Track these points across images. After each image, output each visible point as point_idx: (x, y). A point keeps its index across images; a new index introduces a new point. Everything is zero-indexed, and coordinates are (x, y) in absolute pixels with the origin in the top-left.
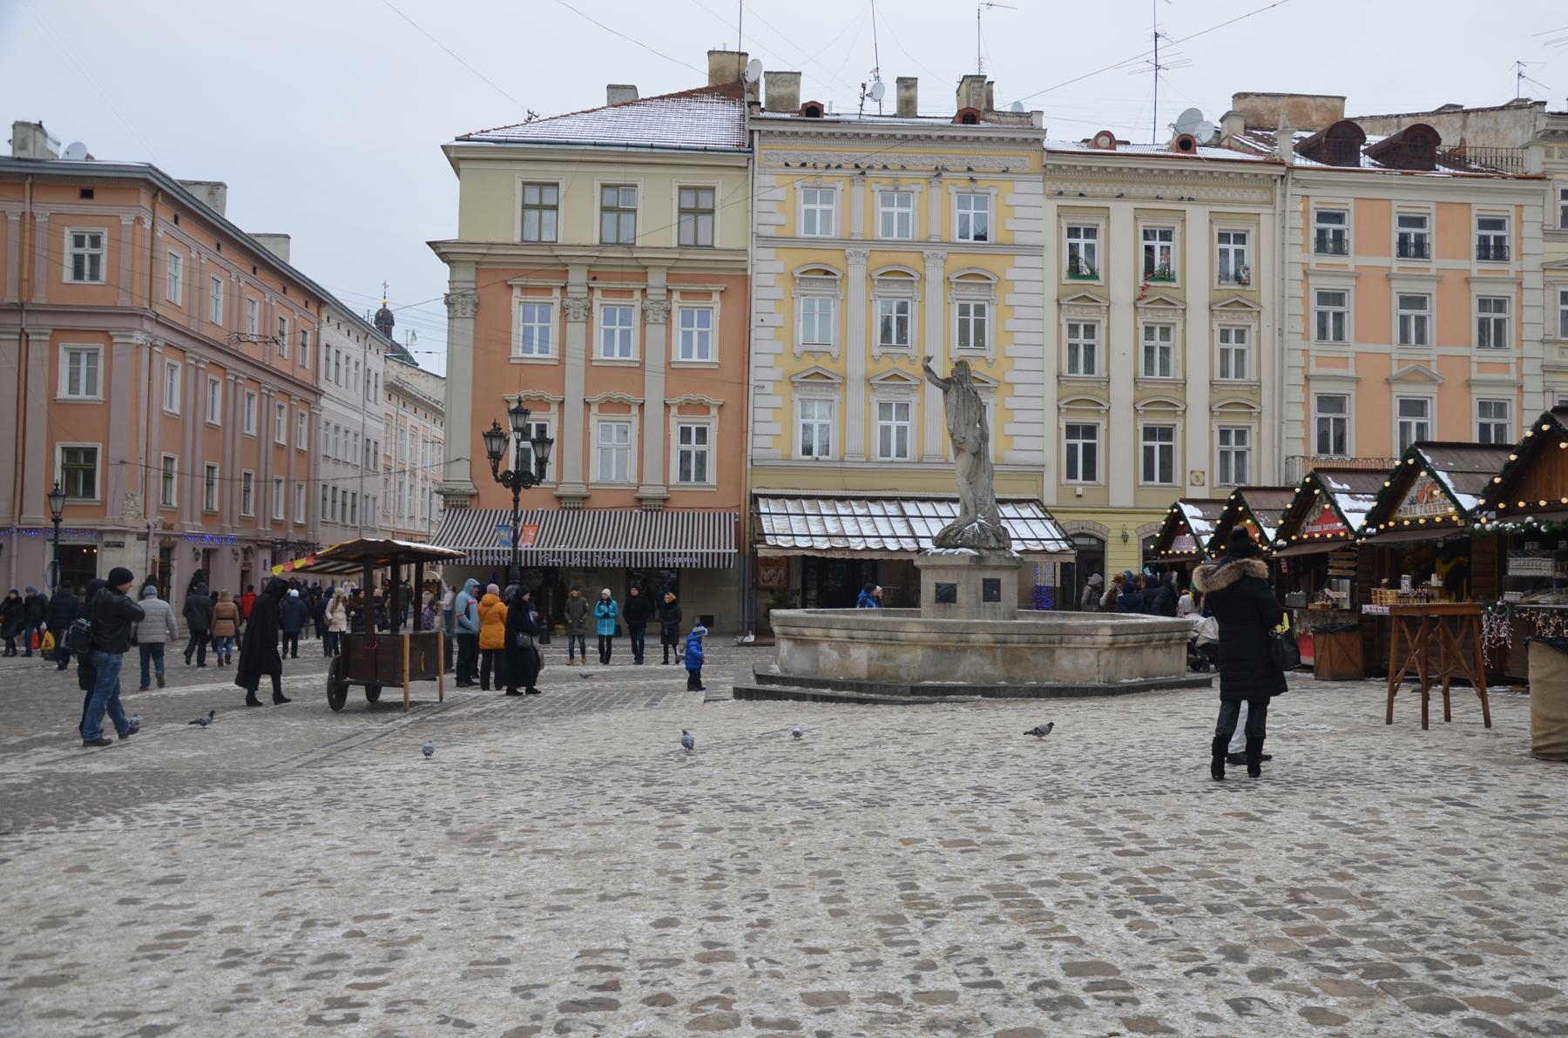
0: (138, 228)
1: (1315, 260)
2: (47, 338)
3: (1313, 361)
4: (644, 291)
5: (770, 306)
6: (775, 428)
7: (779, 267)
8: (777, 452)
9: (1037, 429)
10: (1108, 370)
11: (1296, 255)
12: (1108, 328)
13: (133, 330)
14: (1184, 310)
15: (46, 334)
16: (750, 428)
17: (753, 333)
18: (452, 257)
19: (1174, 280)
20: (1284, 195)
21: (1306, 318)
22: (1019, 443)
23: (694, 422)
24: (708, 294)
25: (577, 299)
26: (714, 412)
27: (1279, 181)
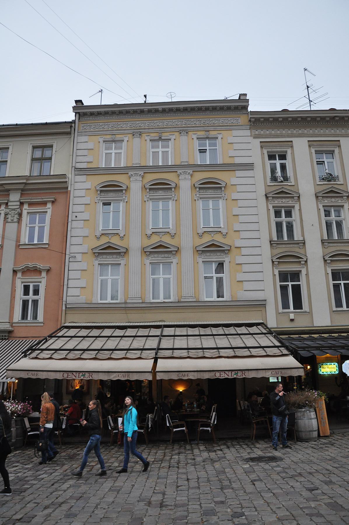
4: (7, 204)
5: (81, 208)
7: (88, 185)
8: (82, 299)
9: (259, 276)
10: (303, 235)
12: (300, 210)
16: (66, 283)
17: (69, 224)
22: (247, 286)
24: (45, 203)
26: (44, 274)
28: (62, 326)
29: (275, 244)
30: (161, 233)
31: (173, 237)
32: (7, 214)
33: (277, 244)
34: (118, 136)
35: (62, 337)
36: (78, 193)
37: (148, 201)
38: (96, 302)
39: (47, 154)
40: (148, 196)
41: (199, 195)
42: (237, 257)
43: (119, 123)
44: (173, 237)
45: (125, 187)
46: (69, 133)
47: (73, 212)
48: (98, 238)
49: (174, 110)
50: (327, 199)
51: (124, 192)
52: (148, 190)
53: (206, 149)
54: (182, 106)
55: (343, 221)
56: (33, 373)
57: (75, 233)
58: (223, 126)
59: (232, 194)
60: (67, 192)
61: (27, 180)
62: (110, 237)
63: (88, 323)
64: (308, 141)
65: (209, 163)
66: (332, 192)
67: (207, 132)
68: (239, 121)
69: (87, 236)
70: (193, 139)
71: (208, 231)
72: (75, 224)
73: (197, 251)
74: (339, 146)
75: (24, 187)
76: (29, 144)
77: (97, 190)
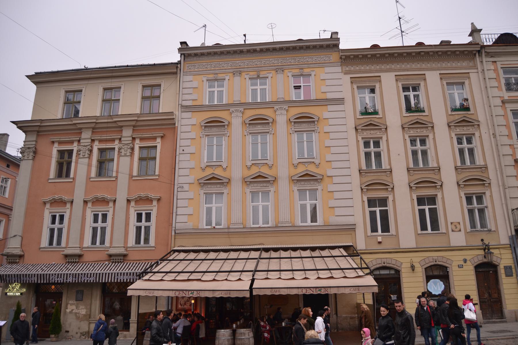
1: (507, 95)
4: (120, 139)
5: (188, 142)
6: (189, 211)
7: (194, 121)
8: (190, 225)
9: (349, 203)
10: (390, 164)
11: (495, 92)
12: (387, 141)
14: (433, 127)
16: (174, 211)
17: (177, 157)
18: (25, 129)
19: (424, 111)
20: (482, 62)
23: (144, 209)
24: (155, 138)
25: (84, 146)
26: (155, 203)
28: (171, 250)
29: (364, 172)
30: (260, 164)
31: (270, 167)
32: (120, 149)
33: (366, 172)
35: (173, 260)
36: (184, 129)
37: (248, 135)
38: (202, 228)
39: (156, 93)
40: (247, 131)
41: (294, 129)
42: (328, 185)
43: (221, 63)
44: (270, 167)
45: (226, 123)
46: (176, 73)
47: (180, 146)
48: (203, 170)
49: (271, 50)
50: (413, 130)
51: (226, 127)
52: (248, 125)
53: (301, 86)
54: (278, 46)
55: (428, 150)
56: (150, 292)
57: (182, 165)
58: (316, 64)
59: (325, 127)
60: (175, 128)
61: (138, 117)
62: (214, 169)
63: (195, 246)
64: (395, 75)
65: (303, 99)
66: (417, 123)
67: (301, 70)
68: (331, 58)
69: (194, 168)
70: (288, 76)
71: (303, 161)
72: (182, 157)
73: (293, 180)
74: (425, 80)
75: (136, 123)
76: (139, 83)
77: (202, 126)
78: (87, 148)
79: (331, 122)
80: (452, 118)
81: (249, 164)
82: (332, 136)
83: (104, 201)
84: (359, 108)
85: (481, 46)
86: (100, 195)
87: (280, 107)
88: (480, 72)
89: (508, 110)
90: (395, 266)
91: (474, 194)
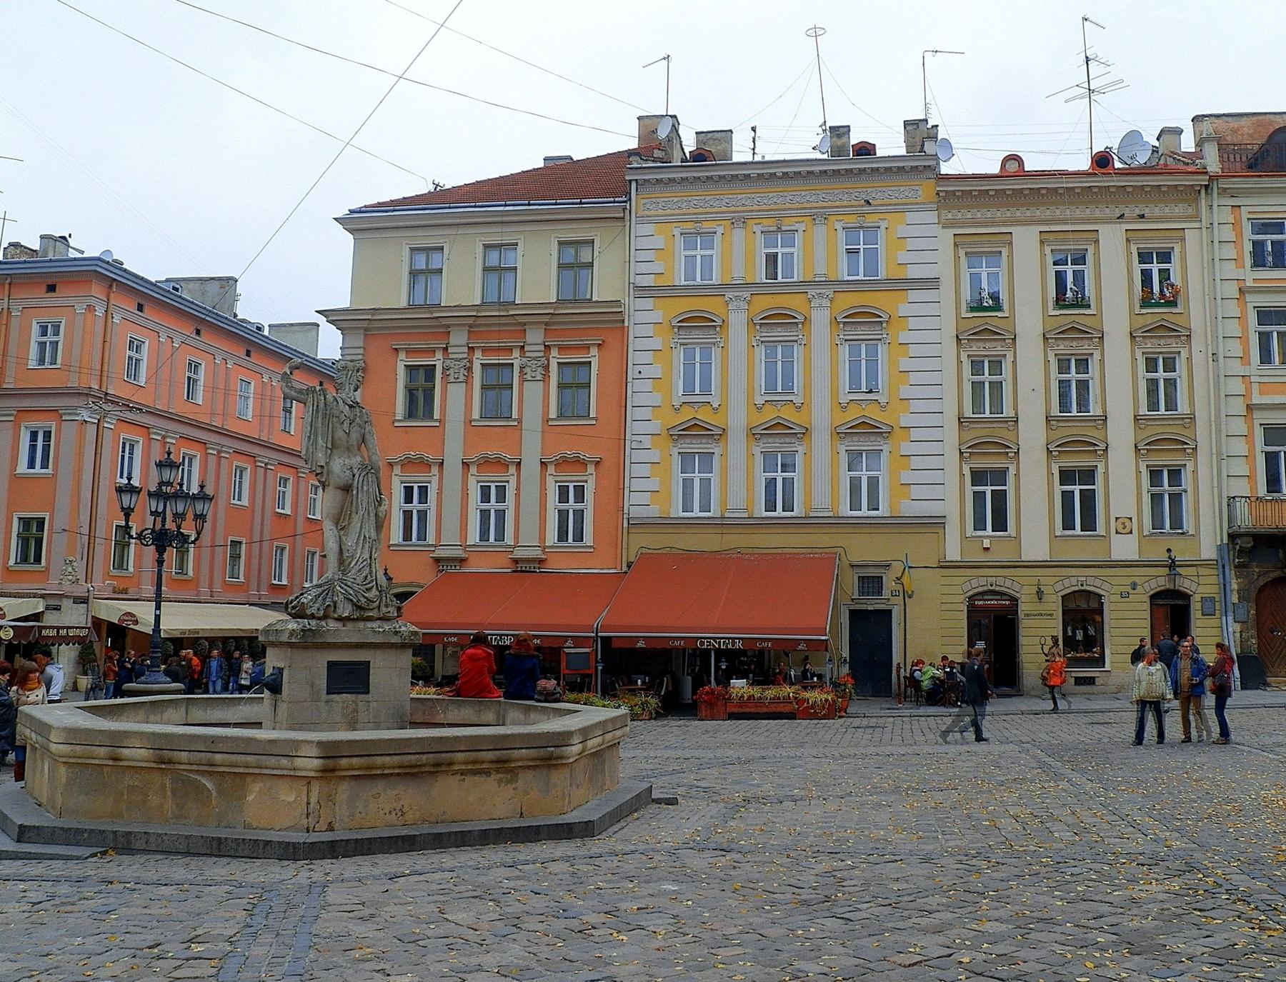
0: (89, 316)
1: (1251, 276)
2: (12, 418)
3: (1255, 386)
5: (648, 357)
6: (653, 484)
7: (657, 316)
8: (654, 511)
10: (1016, 408)
11: (1230, 270)
12: (1014, 362)
13: (77, 408)
14: (1102, 338)
15: (11, 415)
19: (1089, 306)
21: (1243, 339)
22: (916, 492)
25: (456, 360)
26: (591, 469)
27: (1203, 191)
34: (706, 225)
36: (641, 331)
43: (708, 198)
52: (758, 327)
57: (640, 399)
60: (623, 327)
68: (920, 193)
69: (659, 406)
72: (638, 386)
78: (463, 364)
79: (913, 323)
80: (1141, 321)
81: (760, 400)
82: (913, 350)
83: (501, 464)
84: (966, 295)
85: (1210, 176)
86: (491, 453)
87: (818, 291)
88: (1204, 229)
89: (1250, 306)
90: (1012, 592)
91: (1166, 466)
